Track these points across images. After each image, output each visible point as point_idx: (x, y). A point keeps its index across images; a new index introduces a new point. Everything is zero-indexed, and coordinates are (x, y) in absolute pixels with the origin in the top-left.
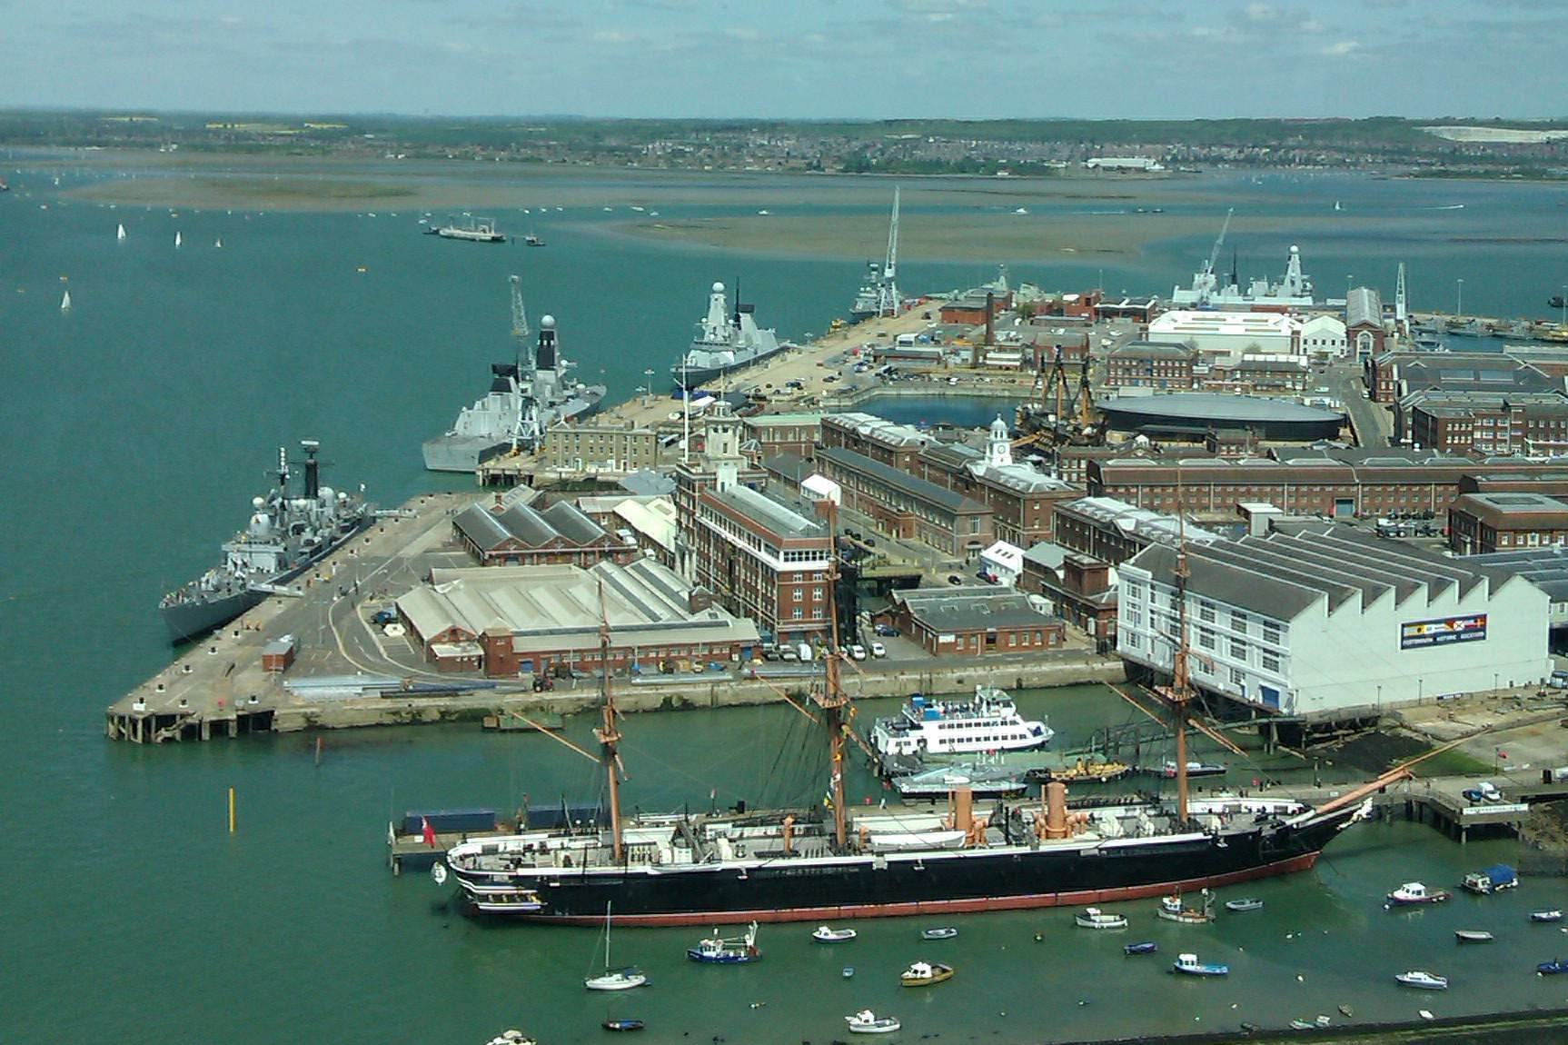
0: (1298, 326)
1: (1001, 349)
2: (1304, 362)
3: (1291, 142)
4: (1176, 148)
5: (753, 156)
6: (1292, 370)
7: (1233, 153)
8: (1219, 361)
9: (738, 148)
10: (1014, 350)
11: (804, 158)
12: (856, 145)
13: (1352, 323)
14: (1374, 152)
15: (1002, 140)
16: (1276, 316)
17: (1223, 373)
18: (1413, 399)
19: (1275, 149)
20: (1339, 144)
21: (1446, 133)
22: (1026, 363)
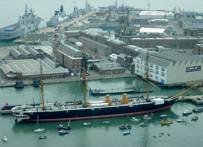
0: (166, 14)
1: (112, 18)
2: (167, 20)
8: (152, 20)
10: (114, 18)
13: (176, 13)
16: (162, 12)
17: (152, 22)
18: (186, 27)
22: (116, 21)
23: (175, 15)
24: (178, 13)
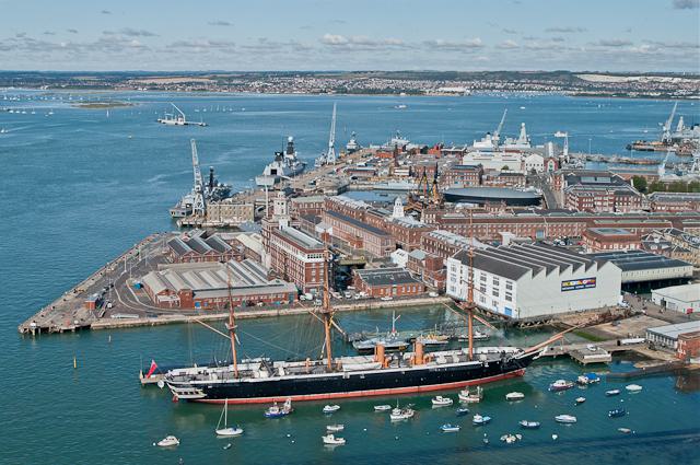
4: (476, 83)
7: (499, 86)
9: (290, 84)
12: (341, 82)
14: (557, 85)
15: (403, 79)
16: (515, 154)
19: (516, 84)
20: (542, 81)
21: (582, 77)
23: (546, 162)
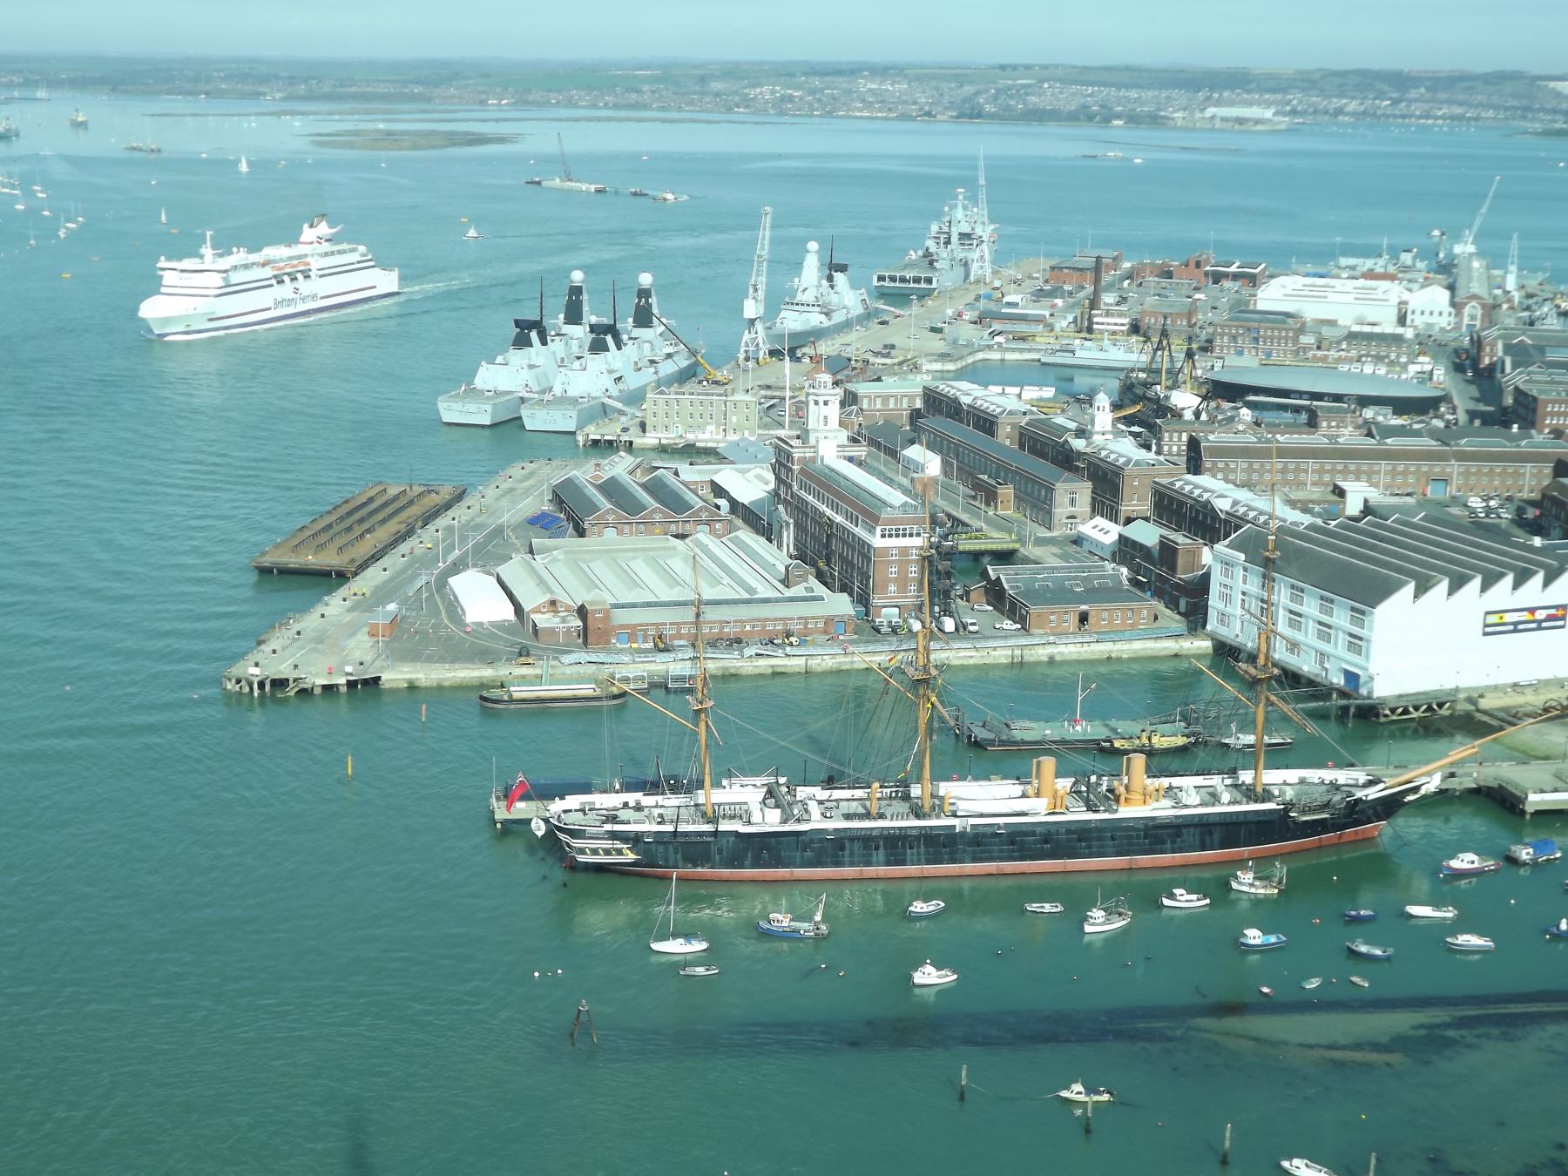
0: (1406, 296)
1: (1108, 314)
2: (1409, 333)
3: (1413, 94)
4: (1295, 98)
5: (863, 101)
6: (1398, 339)
7: (1353, 106)
10: (1121, 314)
11: (915, 103)
12: (968, 89)
14: (1497, 108)
15: (1119, 86)
19: (1395, 102)
20: (1461, 97)
24: (1474, 297)
